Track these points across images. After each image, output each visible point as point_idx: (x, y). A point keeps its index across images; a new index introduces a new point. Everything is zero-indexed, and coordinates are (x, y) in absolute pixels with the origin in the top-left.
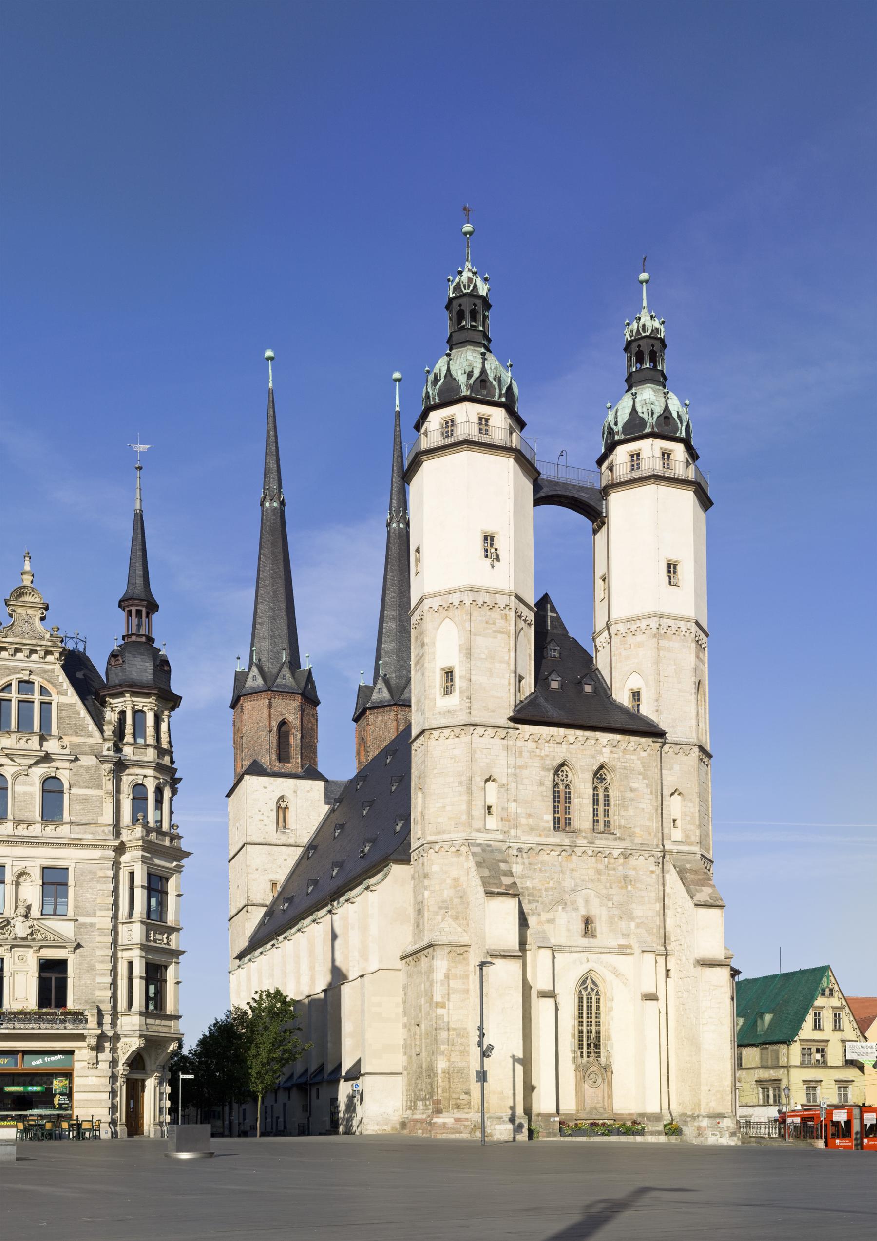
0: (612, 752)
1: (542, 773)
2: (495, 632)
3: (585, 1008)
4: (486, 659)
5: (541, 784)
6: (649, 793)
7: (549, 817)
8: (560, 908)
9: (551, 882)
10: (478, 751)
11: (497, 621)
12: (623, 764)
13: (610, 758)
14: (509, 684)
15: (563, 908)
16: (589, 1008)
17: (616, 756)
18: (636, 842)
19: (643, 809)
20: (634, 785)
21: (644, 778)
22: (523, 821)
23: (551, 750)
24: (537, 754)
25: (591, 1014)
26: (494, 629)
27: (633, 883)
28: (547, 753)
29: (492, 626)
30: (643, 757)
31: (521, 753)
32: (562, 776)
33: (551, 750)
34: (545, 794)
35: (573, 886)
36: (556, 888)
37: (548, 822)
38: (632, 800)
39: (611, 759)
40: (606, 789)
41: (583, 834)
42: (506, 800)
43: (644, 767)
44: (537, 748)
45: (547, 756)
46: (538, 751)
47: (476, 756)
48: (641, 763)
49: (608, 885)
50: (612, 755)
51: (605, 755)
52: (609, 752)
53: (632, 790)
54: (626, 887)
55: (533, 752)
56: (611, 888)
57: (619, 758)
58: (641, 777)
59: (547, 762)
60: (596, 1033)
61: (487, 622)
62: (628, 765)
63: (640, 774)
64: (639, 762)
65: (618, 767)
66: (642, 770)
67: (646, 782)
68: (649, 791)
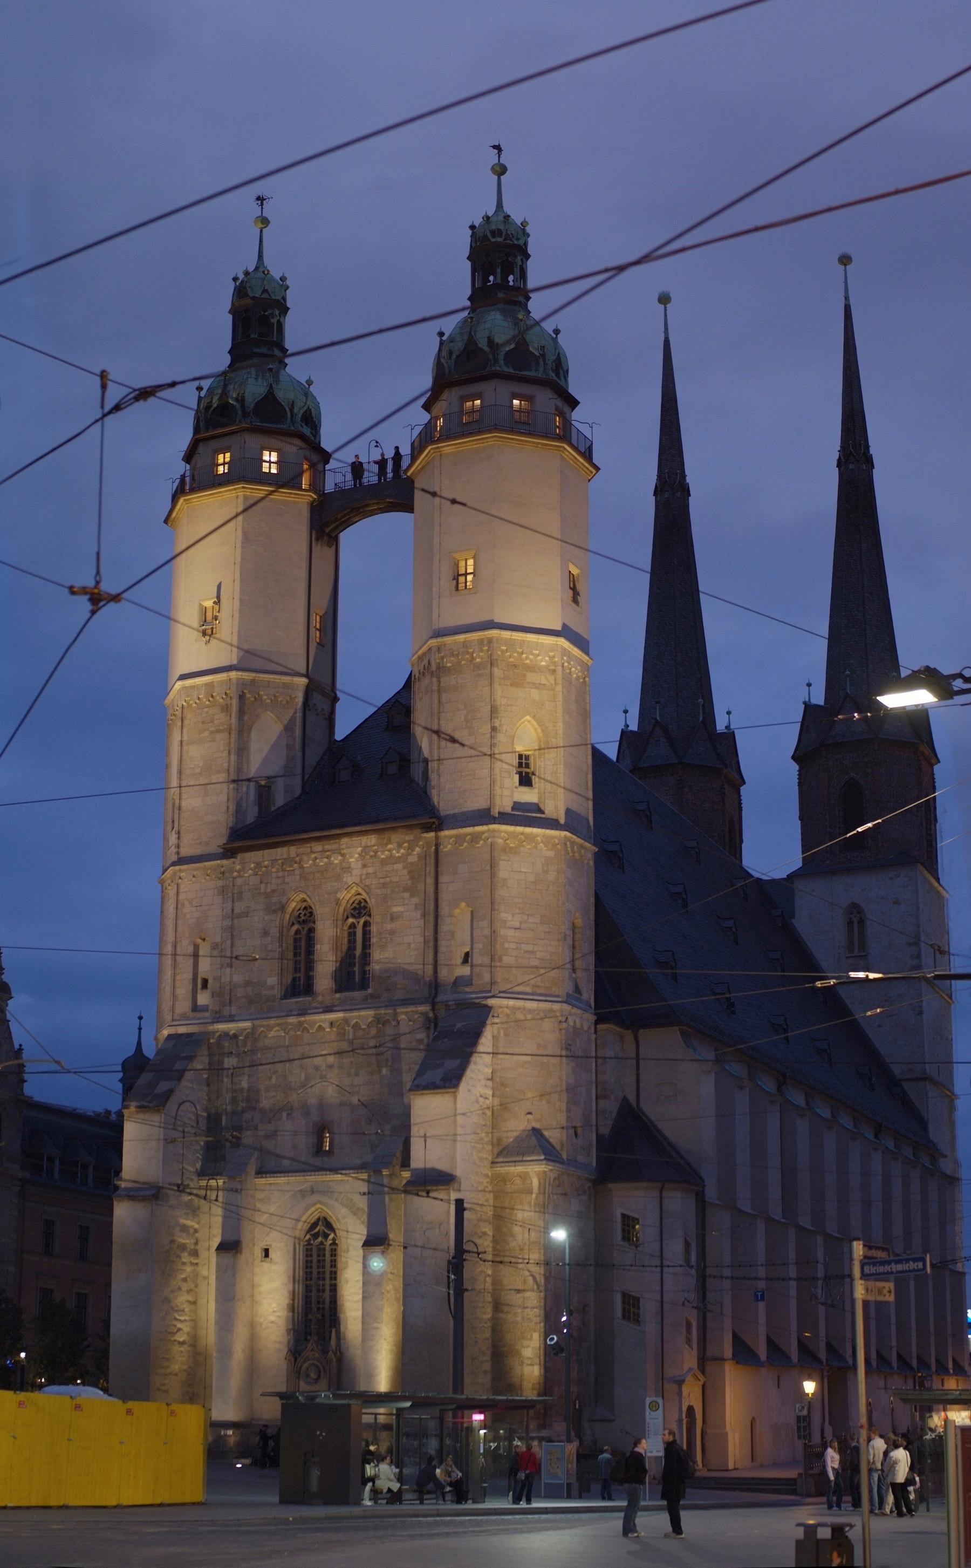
0: (364, 866)
1: (267, 918)
2: (212, 732)
3: (315, 1265)
4: (200, 773)
5: (265, 933)
6: (419, 917)
7: (272, 980)
8: (284, 1114)
9: (274, 1077)
10: (186, 903)
11: (216, 717)
12: (382, 881)
13: (361, 876)
14: (228, 800)
15: (288, 1114)
16: (321, 1264)
17: (371, 870)
18: (396, 998)
19: (409, 944)
20: (395, 909)
21: (412, 896)
22: (240, 992)
23: (280, 881)
24: (262, 891)
25: (324, 1273)
26: (212, 729)
27: (389, 1063)
28: (274, 887)
29: (210, 725)
30: (412, 863)
31: (240, 893)
32: (305, 915)
33: (280, 881)
34: (270, 947)
35: (303, 1078)
36: (279, 1086)
37: (272, 988)
38: (392, 932)
39: (364, 877)
40: (366, 924)
41: (320, 998)
42: (218, 966)
43: (412, 878)
44: (261, 883)
45: (274, 891)
46: (263, 886)
47: (185, 910)
48: (409, 872)
49: (353, 1071)
50: (365, 871)
51: (354, 872)
52: (360, 866)
53: (393, 918)
54: (380, 1071)
55: (256, 889)
56: (357, 1075)
57: (375, 873)
58: (407, 895)
59: (274, 900)
60: (318, 1302)
61: (203, 723)
62: (388, 879)
63: (406, 889)
64: (405, 872)
65: (373, 887)
66: (409, 882)
67: (415, 900)
68: (418, 914)
